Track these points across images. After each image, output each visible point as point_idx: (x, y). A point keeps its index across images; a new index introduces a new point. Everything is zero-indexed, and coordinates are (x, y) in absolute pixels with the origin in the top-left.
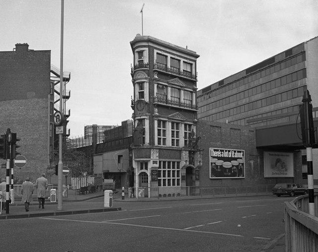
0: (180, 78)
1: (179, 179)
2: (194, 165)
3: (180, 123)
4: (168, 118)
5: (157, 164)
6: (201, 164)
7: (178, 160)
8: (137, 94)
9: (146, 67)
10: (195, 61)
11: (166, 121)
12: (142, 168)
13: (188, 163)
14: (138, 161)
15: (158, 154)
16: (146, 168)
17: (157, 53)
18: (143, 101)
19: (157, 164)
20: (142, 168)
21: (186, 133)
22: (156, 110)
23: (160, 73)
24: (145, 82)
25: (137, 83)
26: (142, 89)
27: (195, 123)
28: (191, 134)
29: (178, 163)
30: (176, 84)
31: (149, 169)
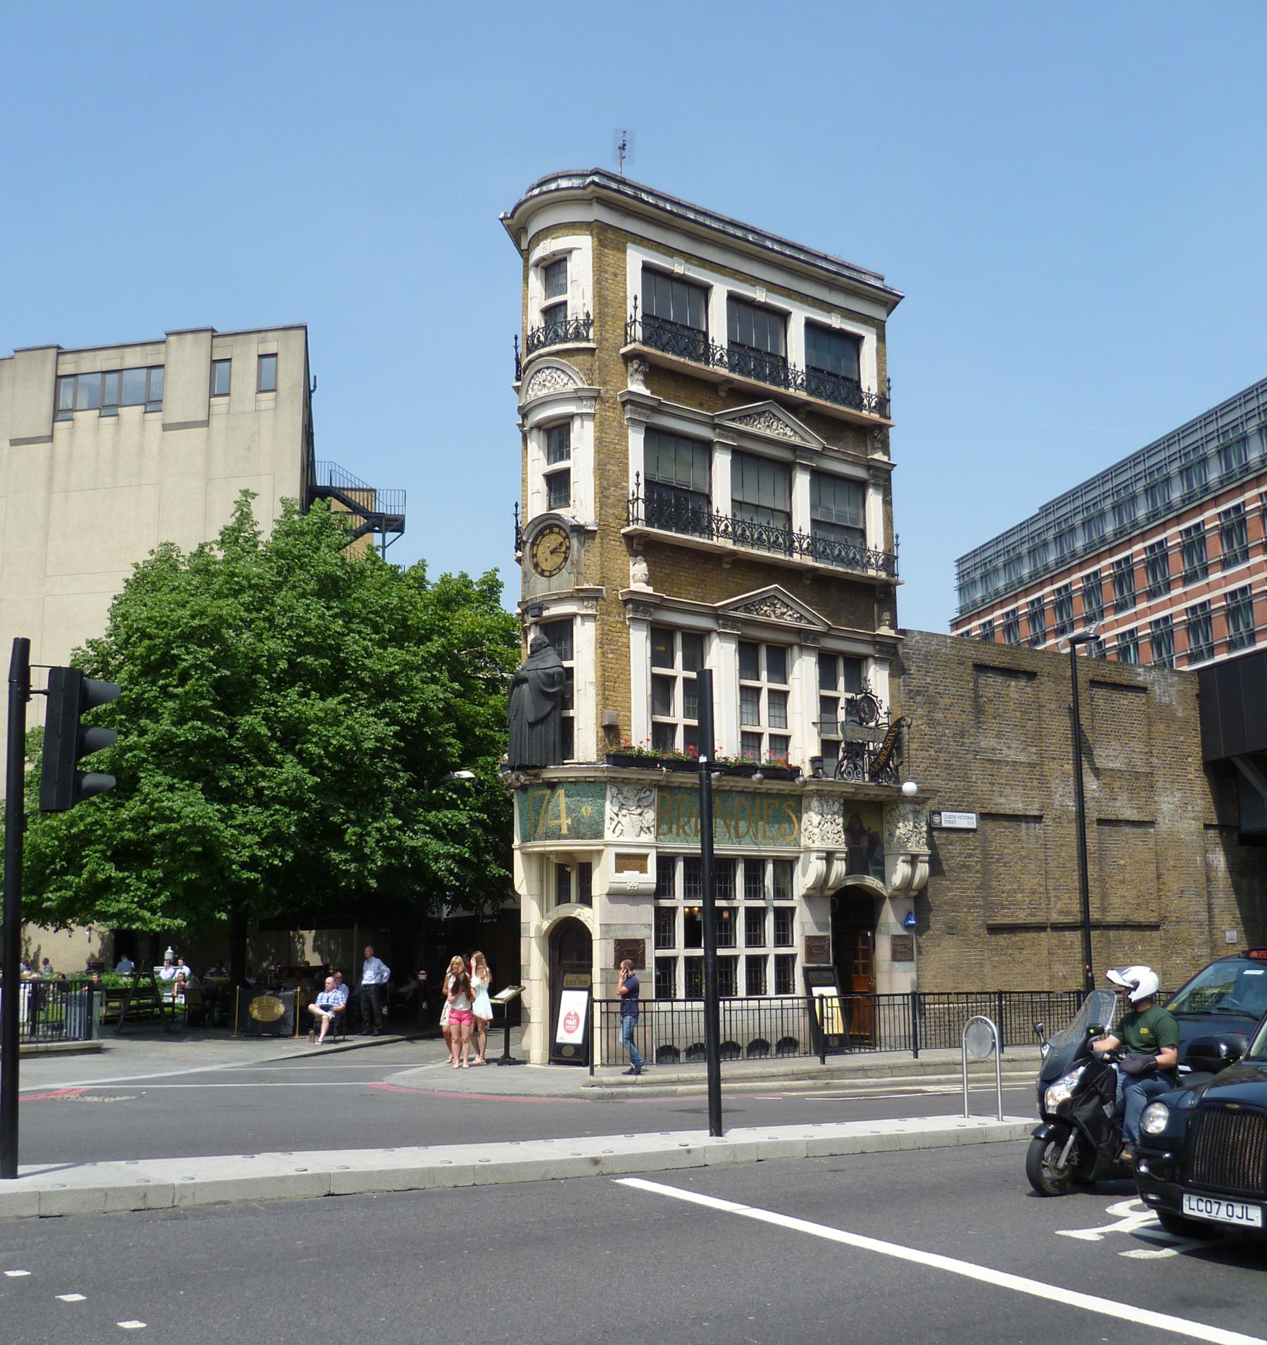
0: (793, 407)
1: (793, 957)
2: (882, 876)
3: (791, 645)
4: (716, 615)
5: (643, 870)
6: (923, 869)
7: (784, 850)
8: (537, 485)
9: (578, 336)
10: (880, 327)
11: (708, 632)
12: (563, 897)
13: (839, 867)
14: (543, 857)
15: (650, 815)
16: (586, 899)
17: (647, 269)
18: (559, 517)
19: (643, 870)
20: (563, 897)
21: (828, 705)
22: (639, 569)
23: (655, 373)
24: (572, 416)
25: (539, 426)
26: (561, 459)
27: (890, 653)
28: (863, 707)
29: (785, 866)
30: (759, 428)
31: (595, 901)
